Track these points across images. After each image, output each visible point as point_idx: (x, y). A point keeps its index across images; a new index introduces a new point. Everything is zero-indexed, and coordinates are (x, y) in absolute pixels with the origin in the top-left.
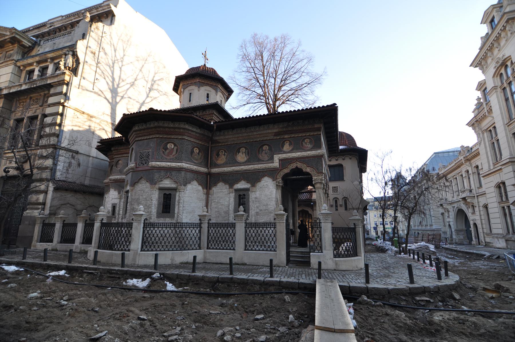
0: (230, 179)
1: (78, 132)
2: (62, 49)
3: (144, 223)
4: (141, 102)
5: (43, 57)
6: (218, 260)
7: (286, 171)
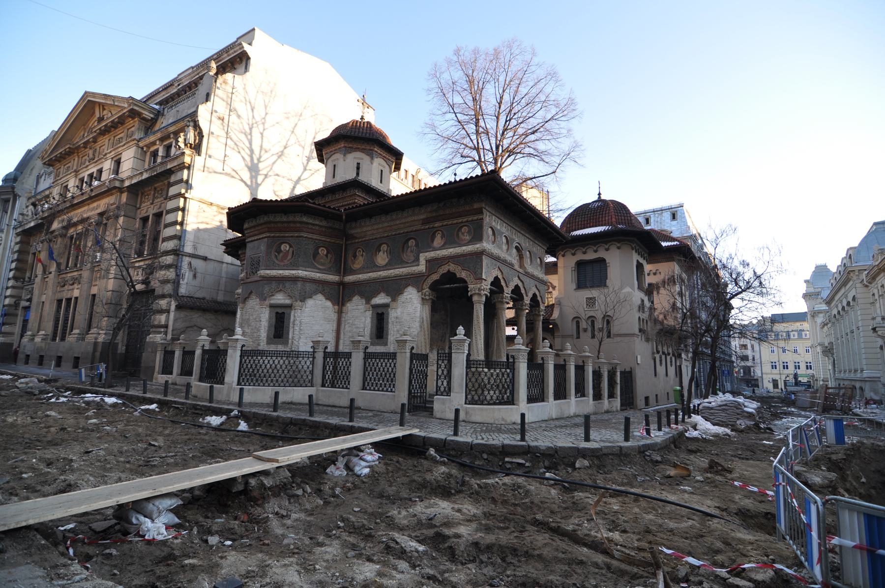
0: (366, 290)
1: (206, 230)
2: (183, 119)
3: (241, 350)
4: (295, 179)
5: (165, 133)
6: (331, 402)
7: (435, 277)
